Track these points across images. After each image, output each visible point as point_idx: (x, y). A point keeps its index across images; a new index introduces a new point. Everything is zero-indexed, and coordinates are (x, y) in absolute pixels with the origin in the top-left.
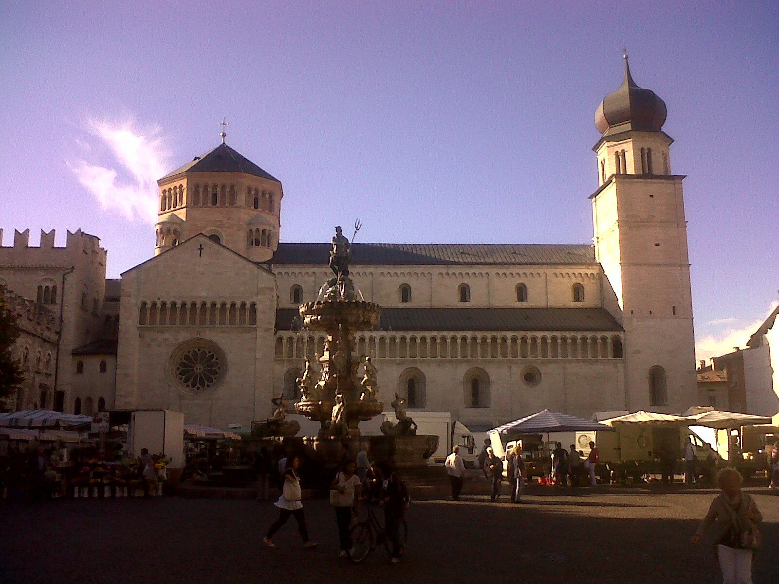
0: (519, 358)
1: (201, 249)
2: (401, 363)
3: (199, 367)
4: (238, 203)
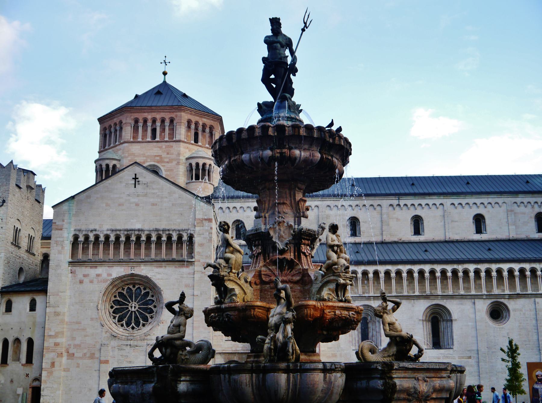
0: (484, 292)
1: (135, 178)
3: (133, 305)
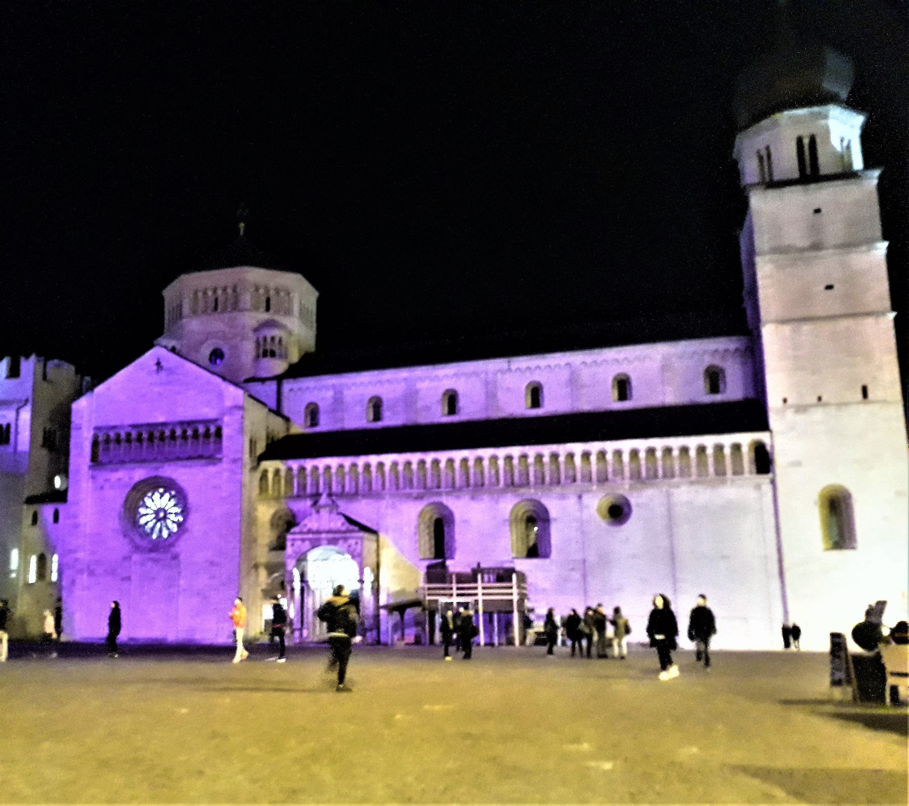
1: (158, 363)
2: (419, 498)
4: (241, 305)
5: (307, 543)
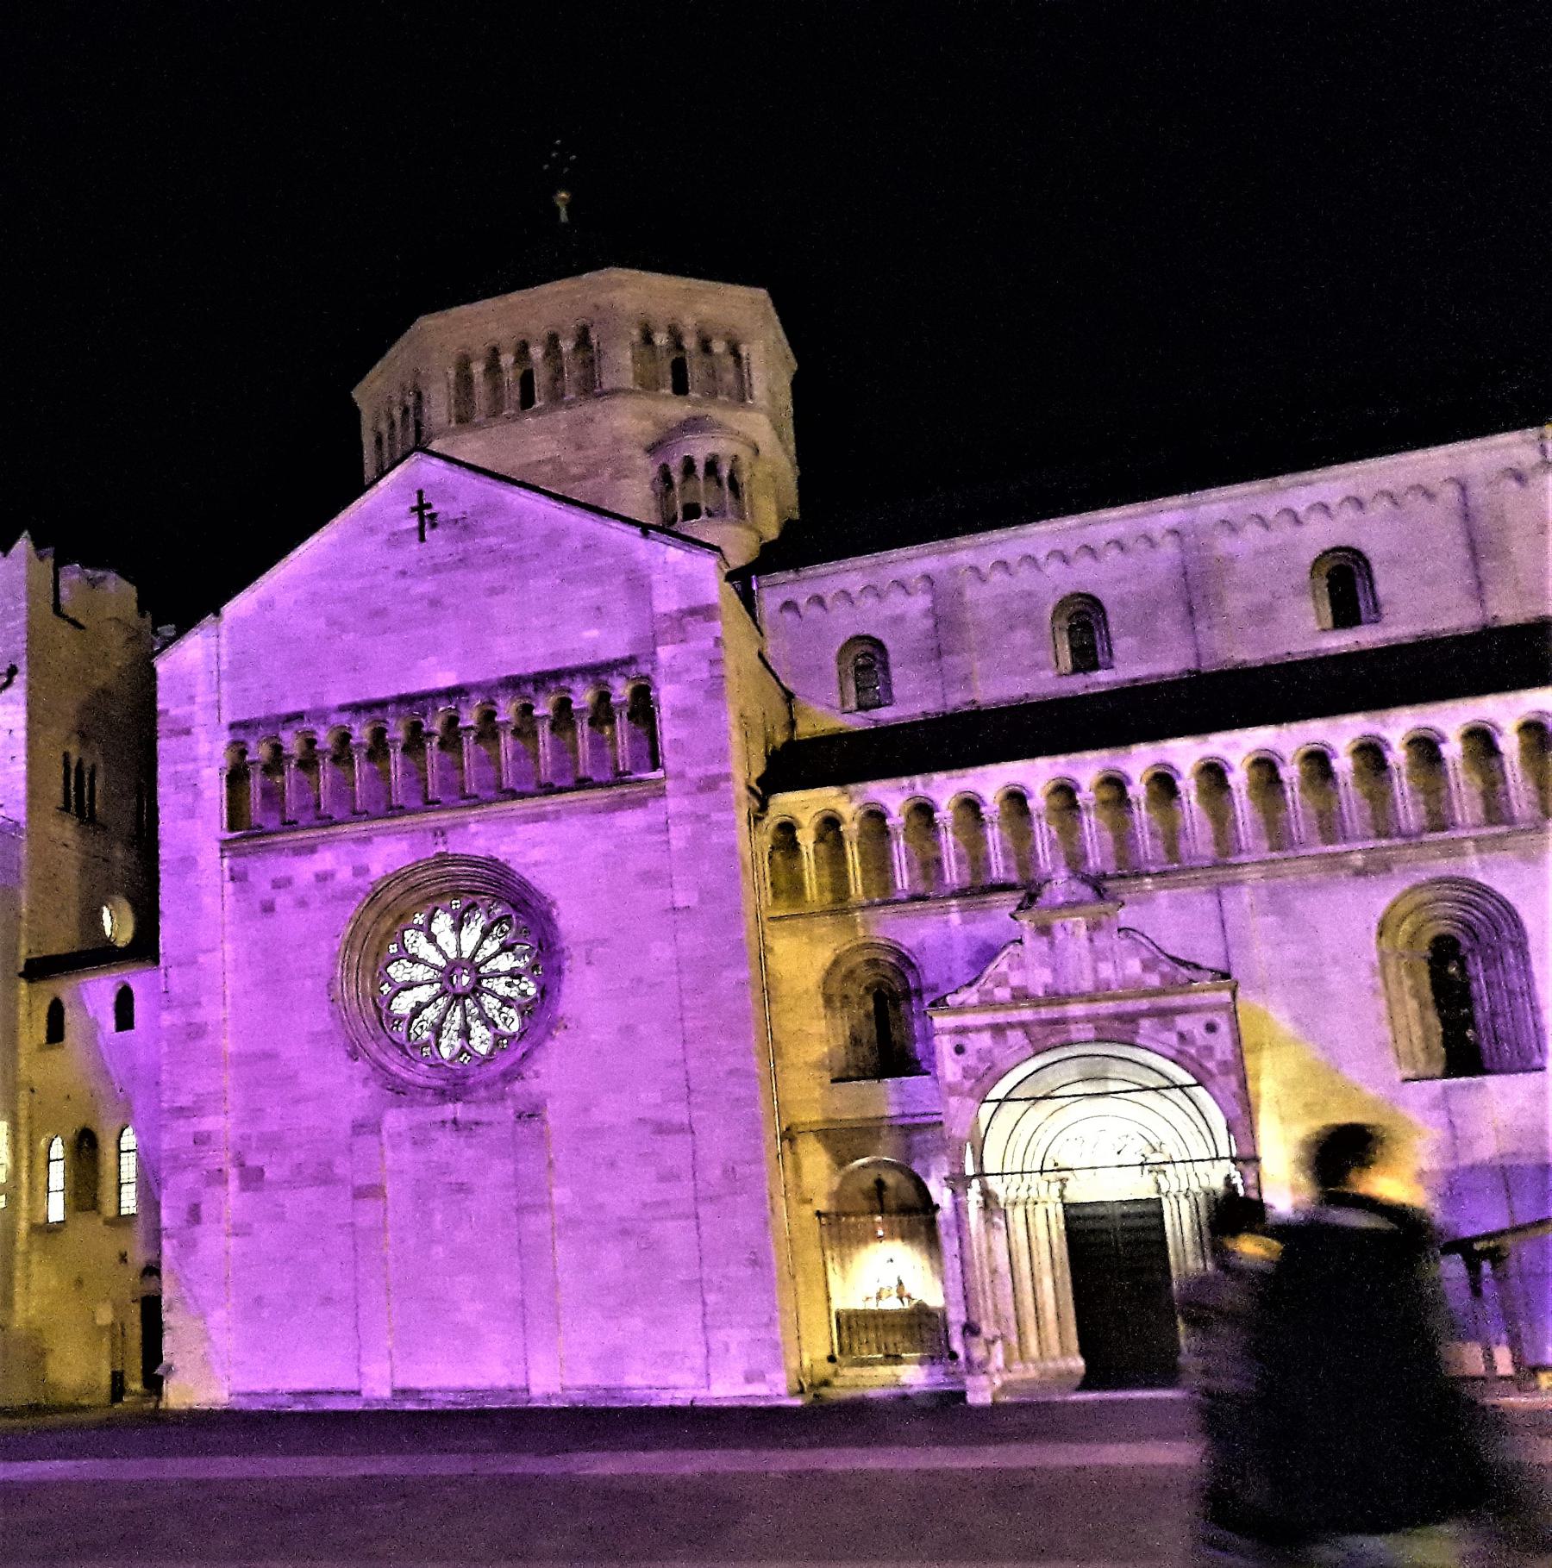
5: (1015, 1037)
